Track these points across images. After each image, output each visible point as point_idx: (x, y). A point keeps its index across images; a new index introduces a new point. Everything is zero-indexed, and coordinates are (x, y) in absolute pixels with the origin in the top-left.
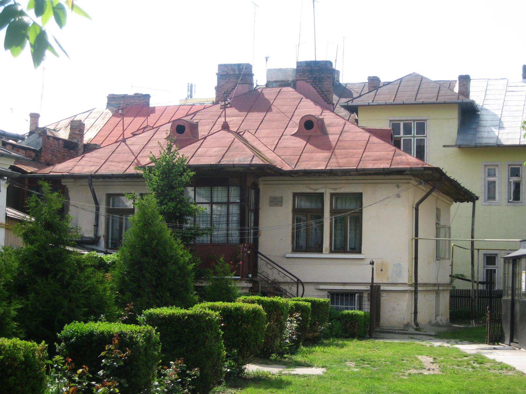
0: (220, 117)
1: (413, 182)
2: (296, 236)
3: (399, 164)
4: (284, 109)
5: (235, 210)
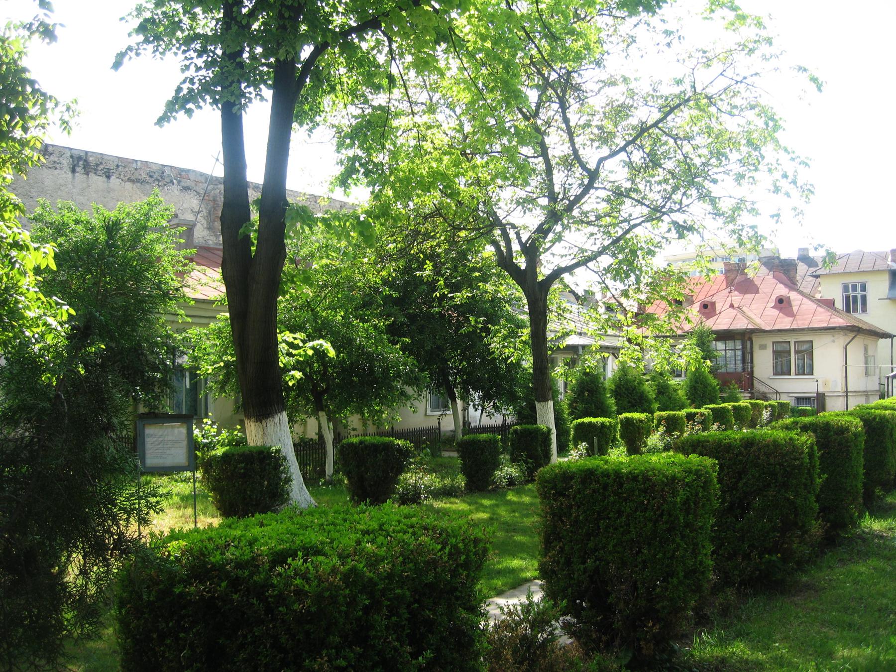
2: (775, 367)
4: (766, 290)
5: (739, 353)
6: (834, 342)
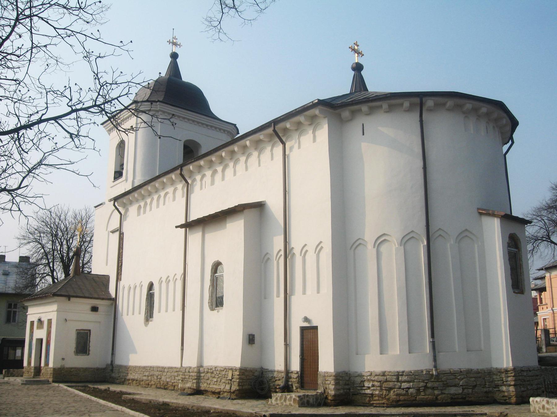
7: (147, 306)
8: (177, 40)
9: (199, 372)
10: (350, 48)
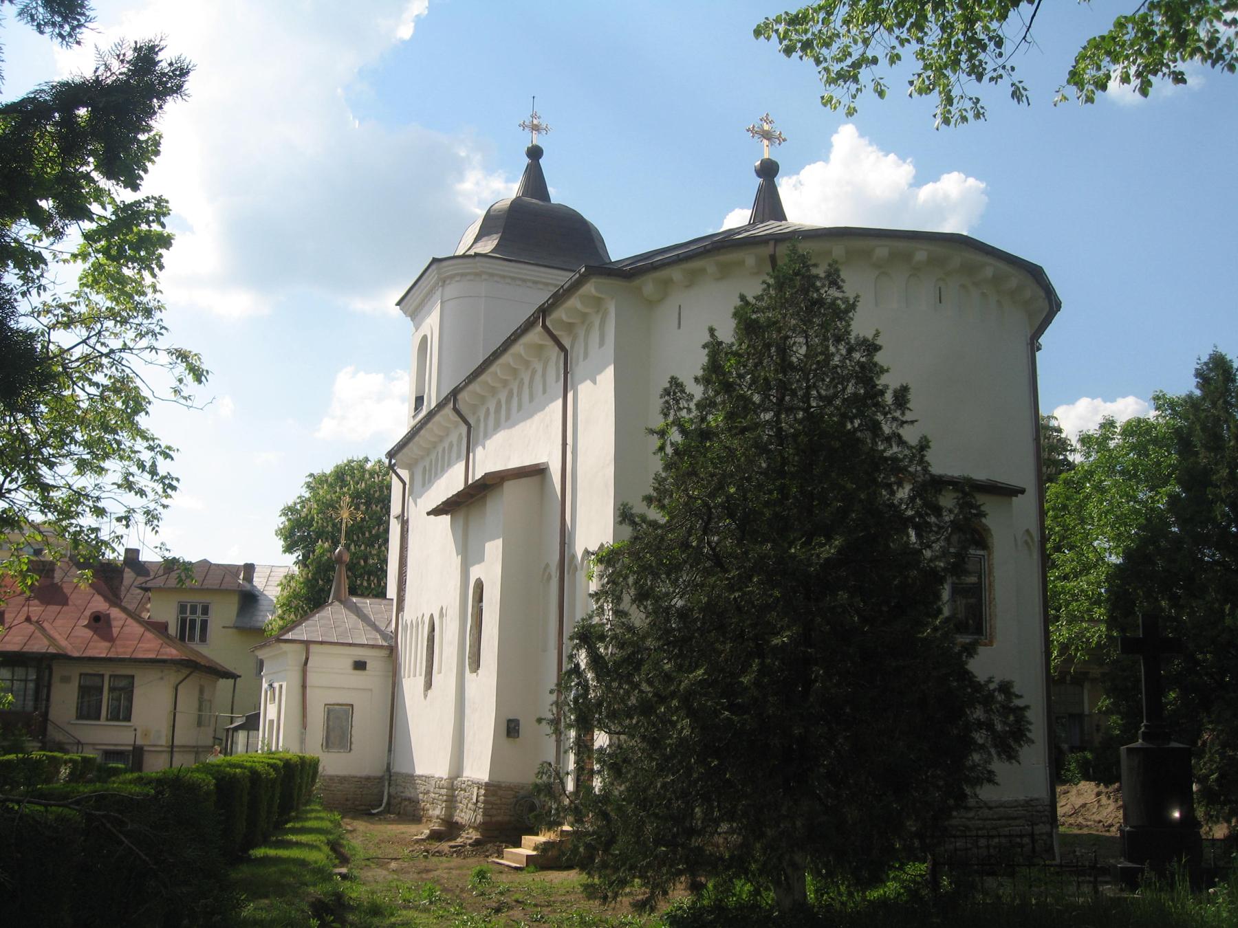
0: (23, 606)
1: (174, 668)
3: (163, 655)
5: (31, 685)
6: (162, 678)
7: (427, 661)
8: (541, 120)
9: (452, 788)
10: (748, 131)
